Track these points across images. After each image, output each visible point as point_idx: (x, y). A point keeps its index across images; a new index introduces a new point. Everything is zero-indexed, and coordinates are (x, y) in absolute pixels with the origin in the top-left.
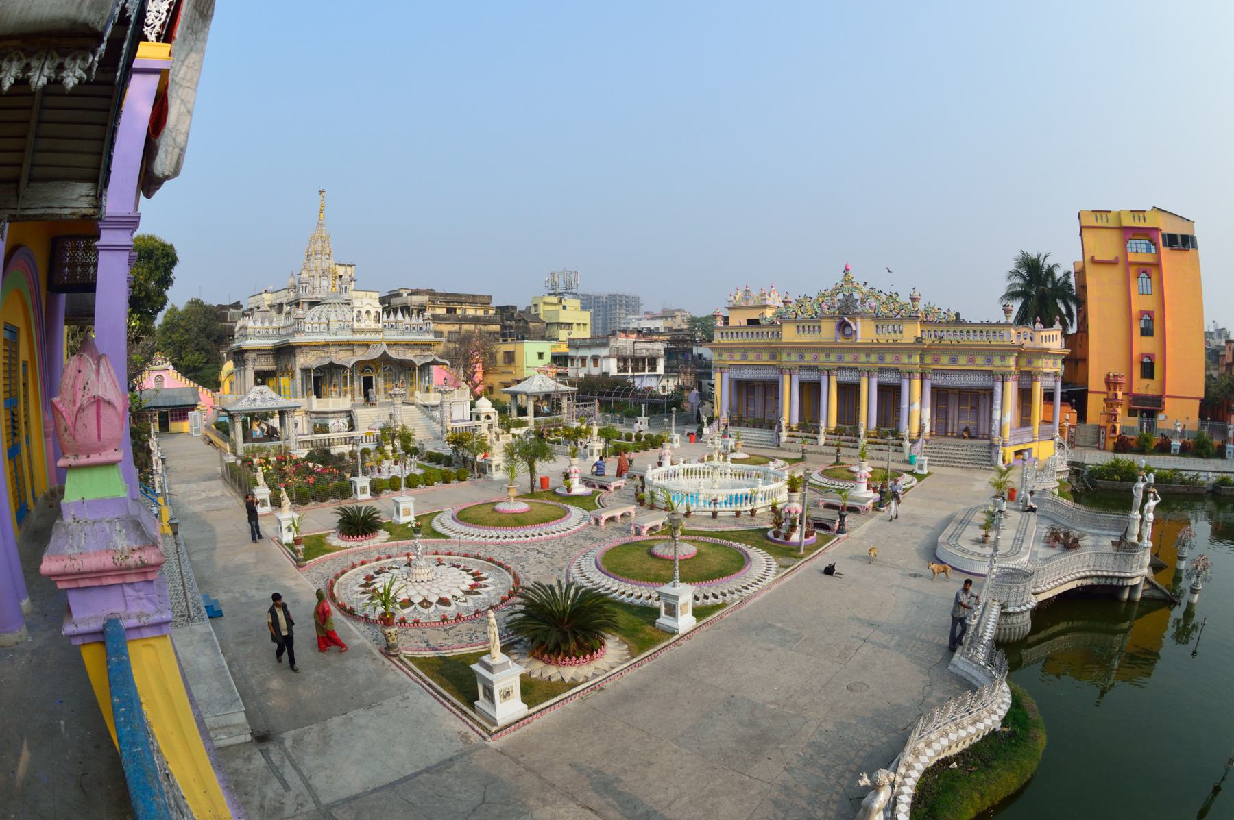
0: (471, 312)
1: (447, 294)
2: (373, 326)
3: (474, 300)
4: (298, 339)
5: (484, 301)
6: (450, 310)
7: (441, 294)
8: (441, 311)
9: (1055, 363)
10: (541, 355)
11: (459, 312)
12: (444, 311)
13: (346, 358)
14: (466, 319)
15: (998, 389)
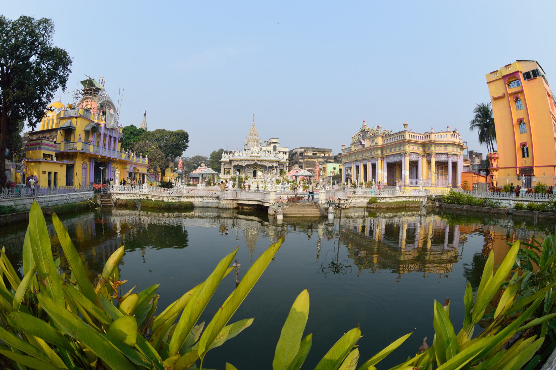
0: (322, 155)
1: (314, 148)
2: (257, 155)
3: (324, 151)
4: (232, 158)
5: (329, 151)
6: (313, 154)
7: (311, 148)
8: (311, 154)
9: (457, 150)
10: (334, 169)
11: (318, 155)
12: (311, 154)
13: (244, 164)
14: (319, 157)
15: (403, 161)
